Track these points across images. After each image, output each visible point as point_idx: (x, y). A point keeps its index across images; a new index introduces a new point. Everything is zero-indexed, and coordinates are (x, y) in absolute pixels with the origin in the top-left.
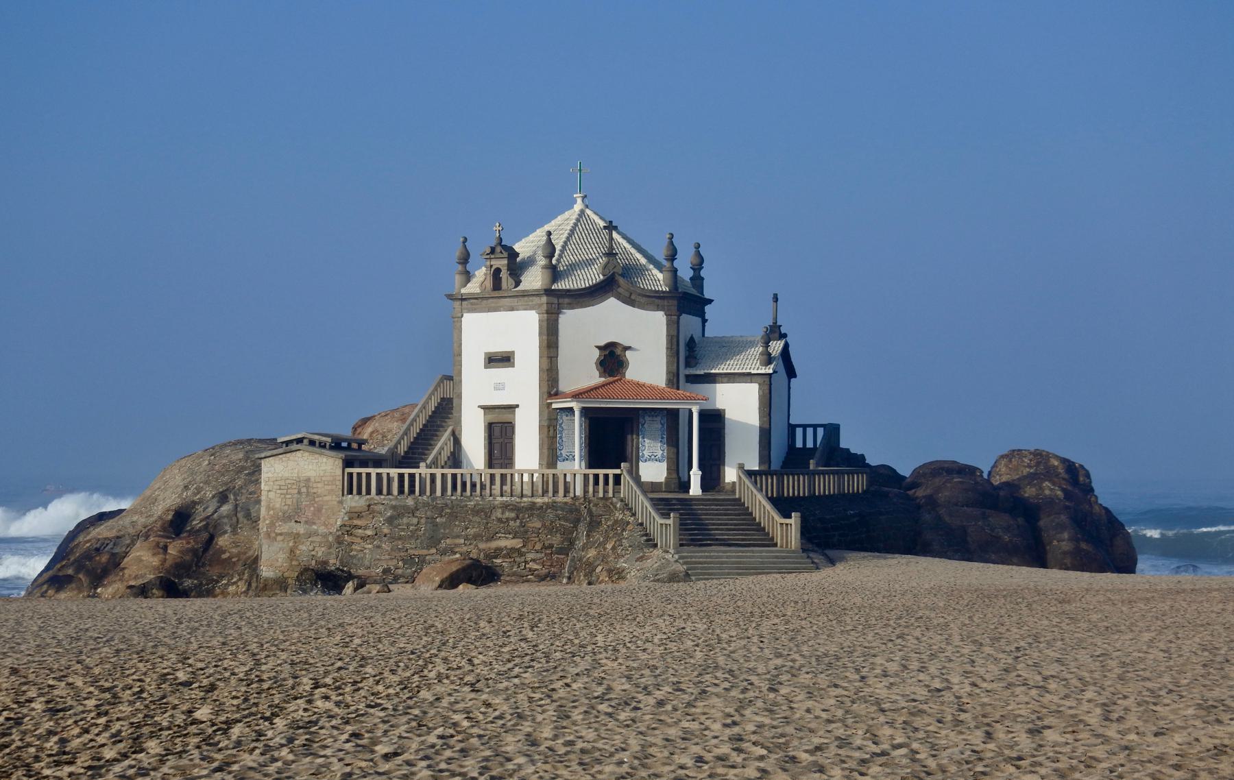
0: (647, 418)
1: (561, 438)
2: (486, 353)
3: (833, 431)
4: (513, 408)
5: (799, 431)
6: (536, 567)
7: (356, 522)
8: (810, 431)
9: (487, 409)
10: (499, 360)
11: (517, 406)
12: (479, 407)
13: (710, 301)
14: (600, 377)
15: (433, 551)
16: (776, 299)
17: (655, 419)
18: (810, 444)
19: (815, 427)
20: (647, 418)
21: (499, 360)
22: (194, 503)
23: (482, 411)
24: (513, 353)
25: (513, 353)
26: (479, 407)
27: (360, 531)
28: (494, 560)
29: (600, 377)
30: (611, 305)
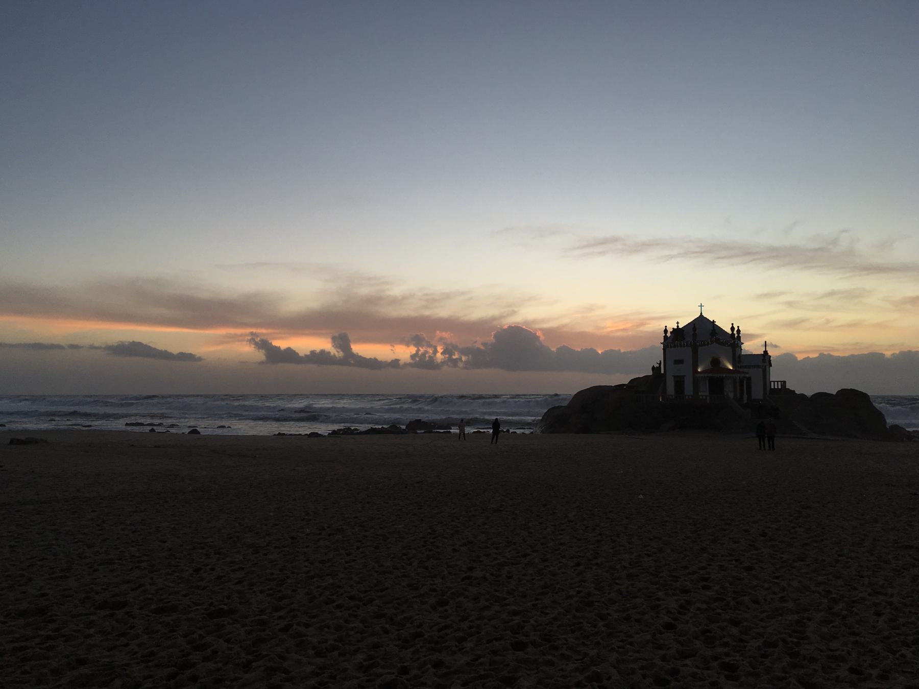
3: (785, 382)
4: (683, 377)
5: (772, 383)
8: (776, 383)
10: (679, 362)
11: (685, 376)
13: (743, 343)
16: (766, 342)
18: (776, 387)
19: (781, 382)
21: (679, 362)
23: (673, 378)
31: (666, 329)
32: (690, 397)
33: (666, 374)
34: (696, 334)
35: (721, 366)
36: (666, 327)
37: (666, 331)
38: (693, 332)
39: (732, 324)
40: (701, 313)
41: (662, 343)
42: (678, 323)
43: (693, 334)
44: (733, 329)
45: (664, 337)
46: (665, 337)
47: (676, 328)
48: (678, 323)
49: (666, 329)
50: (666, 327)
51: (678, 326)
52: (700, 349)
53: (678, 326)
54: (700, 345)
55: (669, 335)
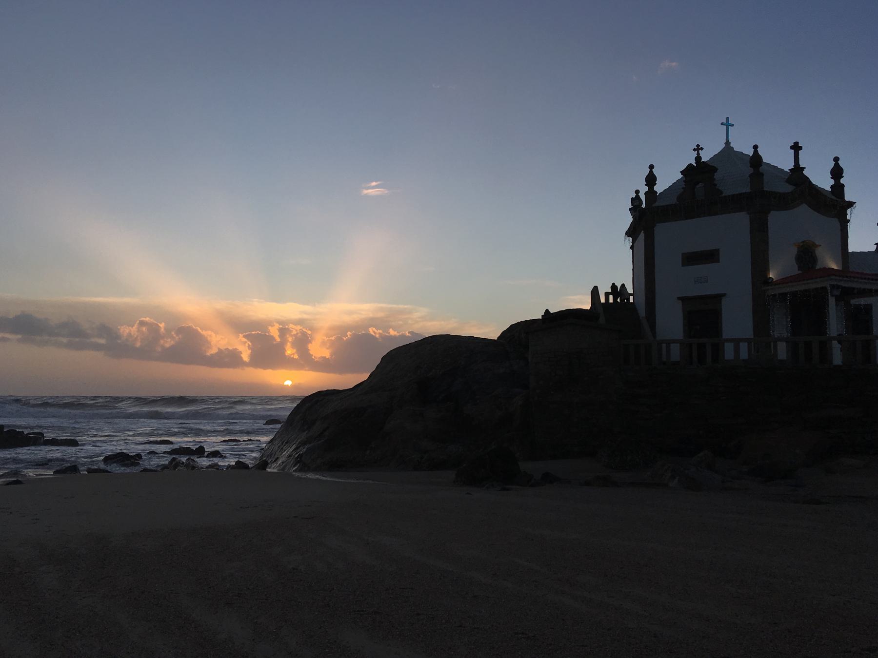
1: (773, 321)
2: (683, 254)
4: (718, 298)
9: (683, 299)
11: (724, 295)
12: (679, 298)
14: (799, 270)
23: (680, 301)
24: (718, 250)
25: (718, 250)
29: (799, 270)
30: (803, 211)
31: (651, 173)
32: (744, 354)
34: (762, 175)
35: (818, 267)
36: (651, 167)
37: (651, 180)
38: (751, 170)
39: (836, 159)
40: (728, 143)
42: (698, 149)
43: (751, 176)
44: (837, 172)
48: (698, 149)
49: (651, 173)
50: (651, 167)
51: (698, 158)
52: (776, 219)
53: (698, 158)
55: (659, 188)
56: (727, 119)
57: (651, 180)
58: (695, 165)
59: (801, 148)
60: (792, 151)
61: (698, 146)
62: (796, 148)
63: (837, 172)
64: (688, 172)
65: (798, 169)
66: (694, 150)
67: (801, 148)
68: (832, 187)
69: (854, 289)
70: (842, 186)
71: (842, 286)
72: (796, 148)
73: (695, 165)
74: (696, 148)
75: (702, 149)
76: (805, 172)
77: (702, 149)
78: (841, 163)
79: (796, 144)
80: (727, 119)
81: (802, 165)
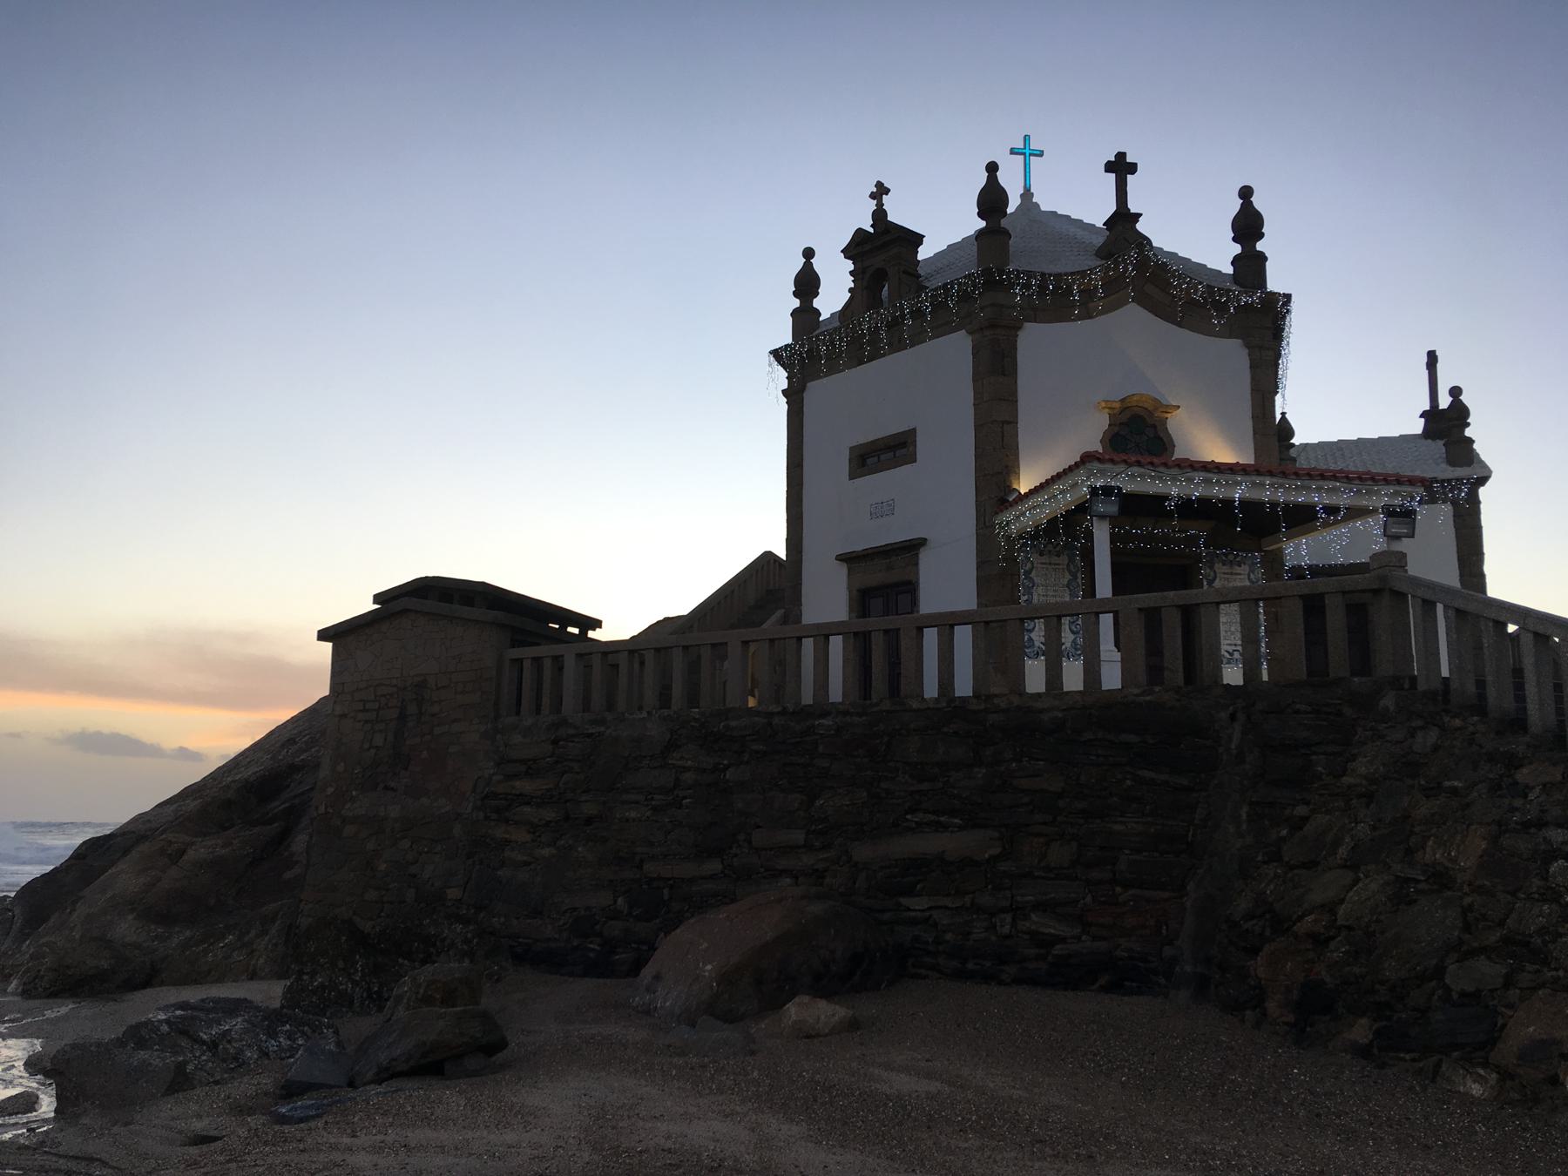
0: (1218, 566)
2: (851, 448)
4: (912, 548)
6: (1051, 927)
7: (525, 786)
11: (921, 542)
12: (841, 558)
15: (714, 866)
16: (1432, 358)
17: (1237, 569)
20: (1218, 566)
22: (294, 768)
23: (842, 571)
26: (841, 558)
27: (527, 809)
28: (905, 901)
30: (1132, 320)
33: (800, 562)
36: (809, 253)
37: (807, 284)
39: (1246, 193)
41: (776, 354)
42: (881, 191)
44: (1248, 226)
45: (794, 313)
46: (804, 317)
47: (867, 225)
48: (881, 191)
50: (809, 253)
51: (879, 215)
53: (879, 215)
54: (1037, 314)
56: (1026, 138)
57: (807, 284)
58: (871, 230)
59: (1132, 168)
60: (1113, 176)
61: (879, 185)
62: (1121, 168)
63: (1248, 226)
64: (858, 248)
65: (1124, 219)
66: (873, 196)
67: (1132, 168)
68: (1236, 261)
69: (1166, 498)
70: (1262, 258)
71: (1120, 489)
72: (1121, 168)
73: (871, 230)
74: (875, 190)
75: (887, 191)
76: (1140, 226)
77: (887, 191)
78: (1257, 201)
79: (1121, 156)
80: (1026, 138)
81: (1133, 208)
